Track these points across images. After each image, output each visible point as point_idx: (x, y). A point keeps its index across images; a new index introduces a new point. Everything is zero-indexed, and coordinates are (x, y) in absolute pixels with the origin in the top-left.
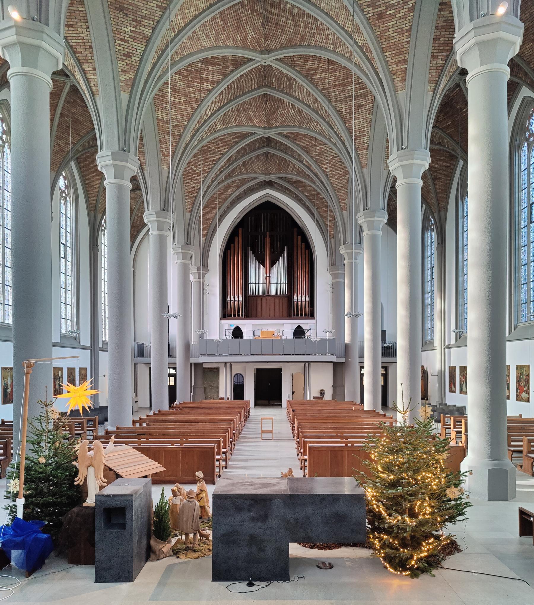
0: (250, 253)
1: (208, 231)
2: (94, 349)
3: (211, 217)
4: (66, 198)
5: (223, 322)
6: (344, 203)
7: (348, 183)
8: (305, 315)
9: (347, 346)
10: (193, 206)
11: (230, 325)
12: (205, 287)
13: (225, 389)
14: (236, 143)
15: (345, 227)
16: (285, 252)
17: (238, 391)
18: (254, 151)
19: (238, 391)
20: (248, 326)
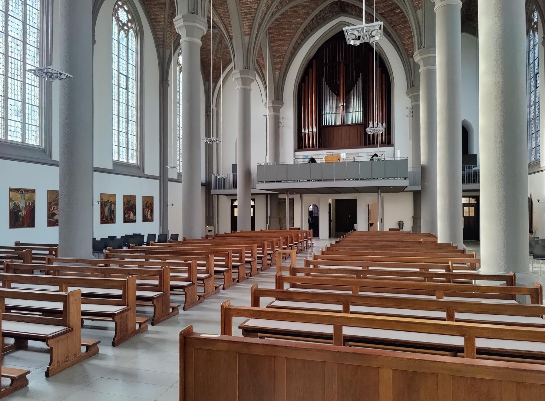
0: (324, 83)
1: (281, 64)
2: (163, 179)
3: (284, 50)
4: (128, 32)
5: (298, 153)
8: (382, 143)
9: (423, 168)
10: (251, 29)
11: (303, 156)
12: (280, 120)
13: (300, 221)
15: (420, 31)
16: (360, 79)
17: (314, 222)
19: (314, 222)
20: (320, 155)
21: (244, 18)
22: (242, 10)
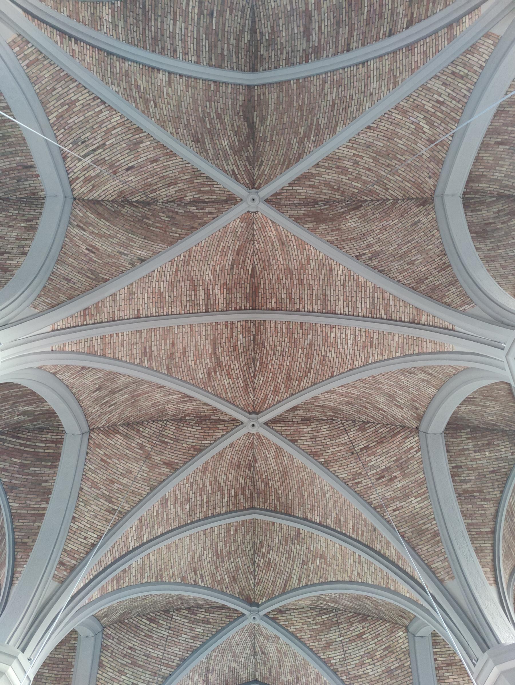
6: (26, 57)
7: (44, 104)
14: (317, 165)
18: (280, 84)
21: (475, 72)
22: (469, 90)
